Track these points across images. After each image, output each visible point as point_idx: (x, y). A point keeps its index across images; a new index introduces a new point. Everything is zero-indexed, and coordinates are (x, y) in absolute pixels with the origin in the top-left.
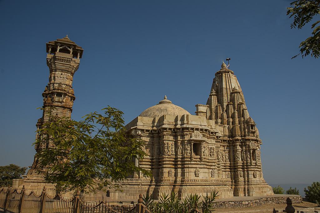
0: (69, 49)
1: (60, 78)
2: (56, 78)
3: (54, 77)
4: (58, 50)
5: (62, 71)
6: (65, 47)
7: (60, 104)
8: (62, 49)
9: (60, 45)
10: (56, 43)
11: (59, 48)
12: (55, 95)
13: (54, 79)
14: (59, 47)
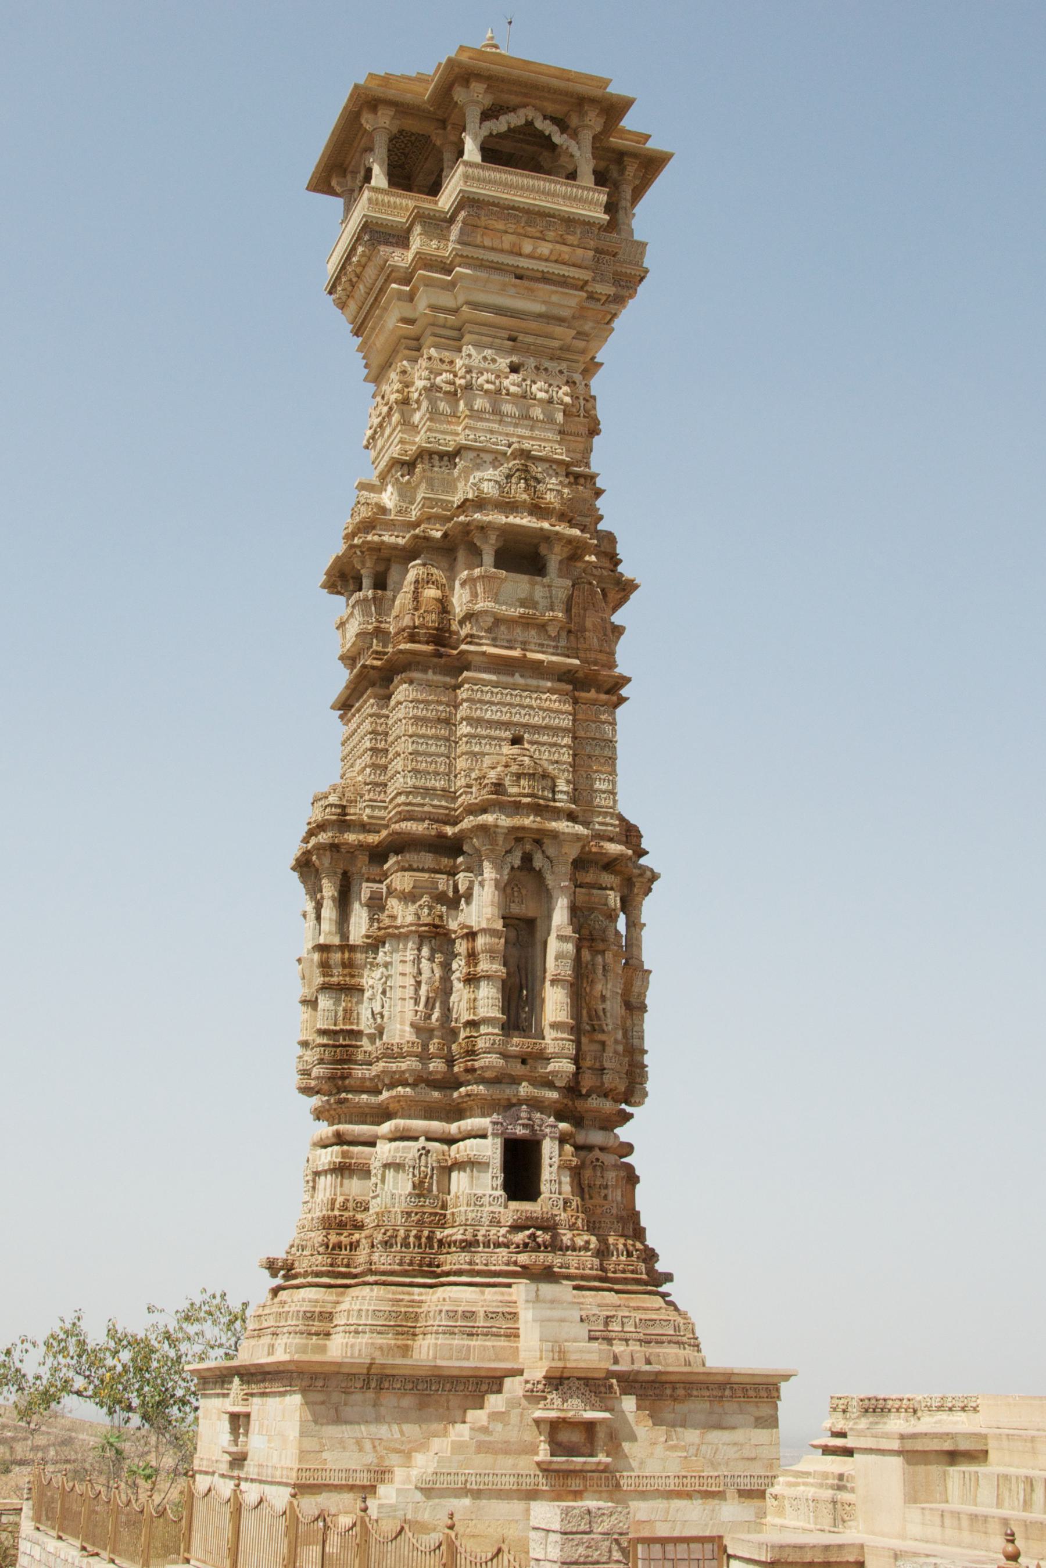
0: (558, 139)
4: (471, 151)
6: (530, 124)
8: (499, 135)
9: (487, 101)
12: (488, 558)
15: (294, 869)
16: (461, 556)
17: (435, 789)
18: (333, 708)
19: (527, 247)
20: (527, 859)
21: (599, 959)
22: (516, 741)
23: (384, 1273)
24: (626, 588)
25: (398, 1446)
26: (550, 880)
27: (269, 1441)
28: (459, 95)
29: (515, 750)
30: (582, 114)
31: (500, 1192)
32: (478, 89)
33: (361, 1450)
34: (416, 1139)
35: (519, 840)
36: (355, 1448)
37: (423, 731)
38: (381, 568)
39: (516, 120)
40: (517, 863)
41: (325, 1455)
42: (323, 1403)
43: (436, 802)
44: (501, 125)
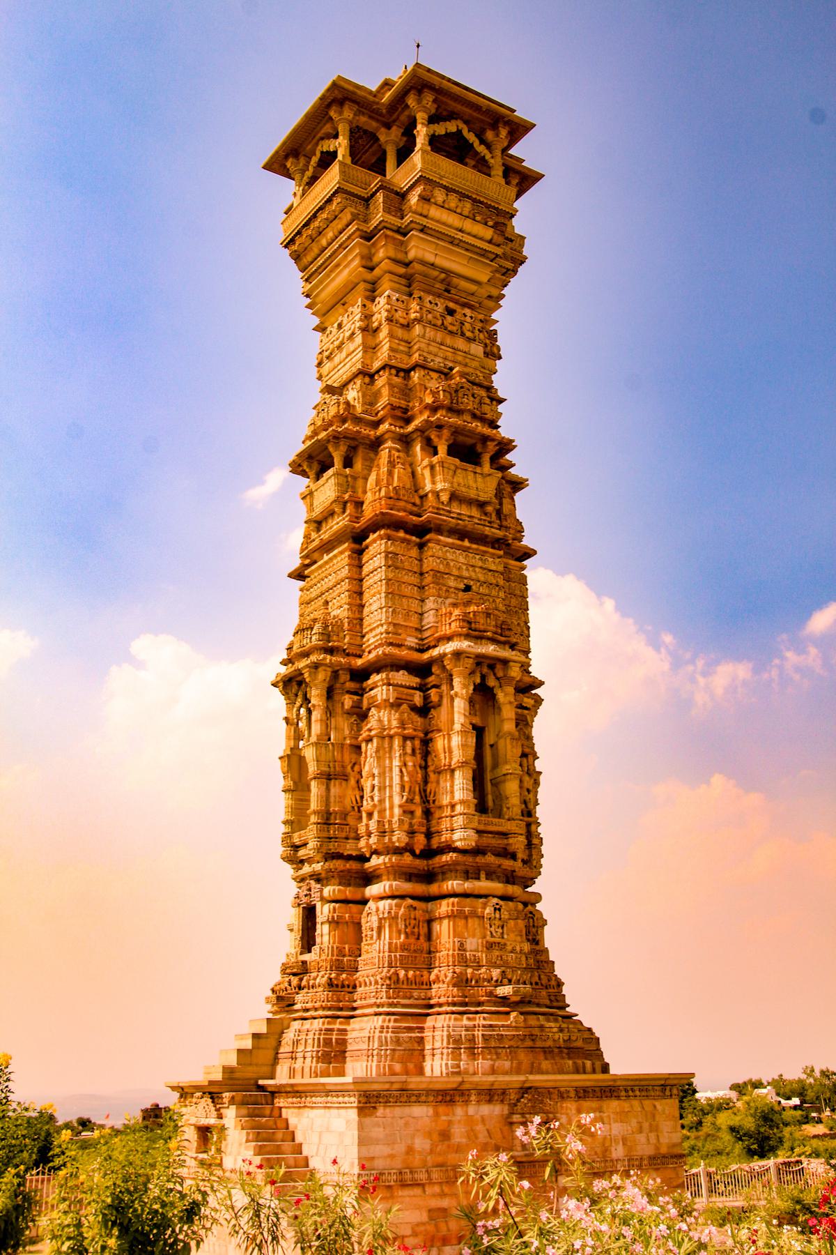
6: (459, 132)
12: (442, 449)
20: (483, 677)
24: (518, 485)
26: (501, 696)
32: (428, 98)
39: (452, 127)
40: (478, 681)
44: (440, 129)
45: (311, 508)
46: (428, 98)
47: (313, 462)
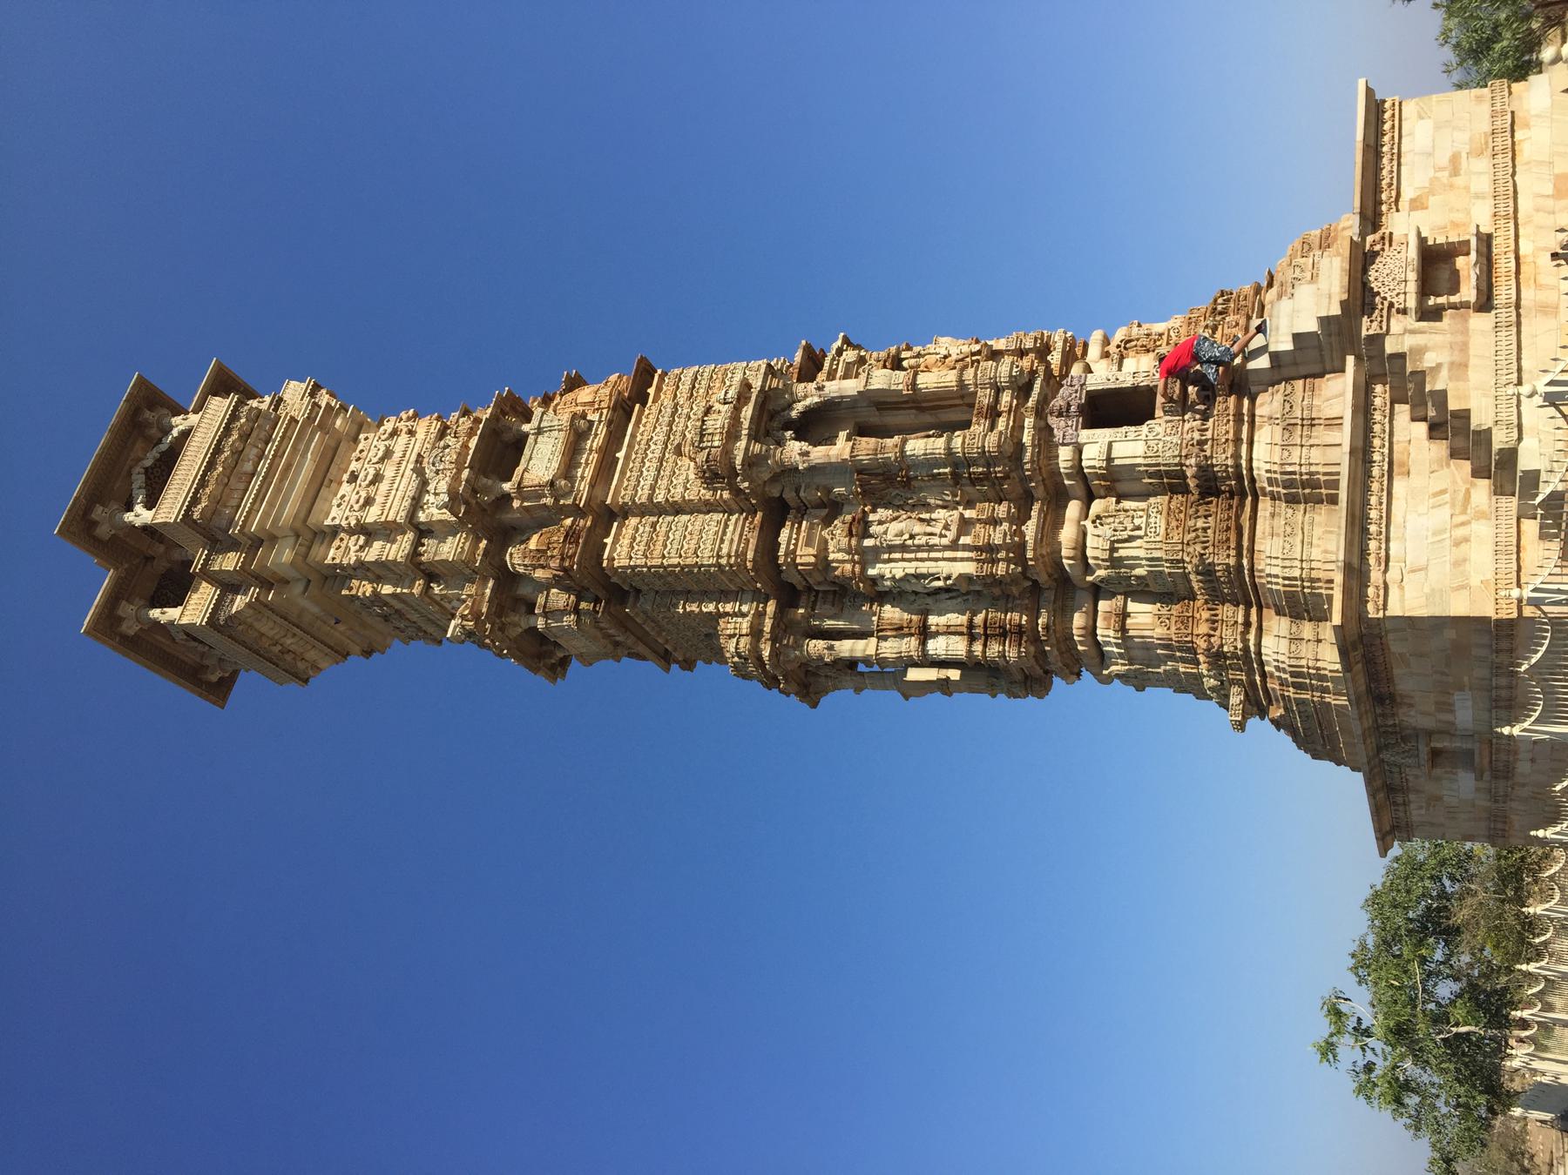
0: (163, 447)
1: (383, 487)
2: (372, 515)
3: (369, 532)
5: (323, 481)
7: (596, 441)
10: (82, 527)
11: (141, 515)
13: (387, 531)
14: (129, 517)
15: (814, 705)
16: (507, 517)
17: (716, 533)
18: (667, 670)
19: (248, 467)
21: (905, 364)
22: (678, 451)
23: (1239, 556)
25: (1461, 496)
27: (1461, 689)
28: (103, 531)
29: (686, 449)
30: (148, 425)
31: (1144, 428)
32: (98, 512)
33: (1467, 540)
34: (1085, 534)
35: (767, 434)
36: (1464, 546)
37: (659, 547)
38: (523, 609)
39: (139, 480)
41: (1475, 581)
42: (1401, 588)
43: (731, 528)
45: (598, 657)
46: (98, 512)
47: (544, 654)
